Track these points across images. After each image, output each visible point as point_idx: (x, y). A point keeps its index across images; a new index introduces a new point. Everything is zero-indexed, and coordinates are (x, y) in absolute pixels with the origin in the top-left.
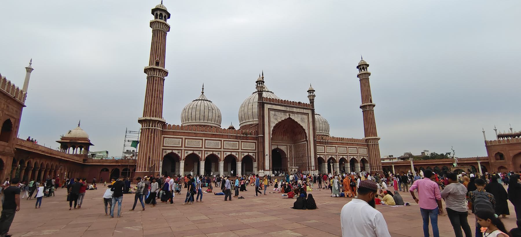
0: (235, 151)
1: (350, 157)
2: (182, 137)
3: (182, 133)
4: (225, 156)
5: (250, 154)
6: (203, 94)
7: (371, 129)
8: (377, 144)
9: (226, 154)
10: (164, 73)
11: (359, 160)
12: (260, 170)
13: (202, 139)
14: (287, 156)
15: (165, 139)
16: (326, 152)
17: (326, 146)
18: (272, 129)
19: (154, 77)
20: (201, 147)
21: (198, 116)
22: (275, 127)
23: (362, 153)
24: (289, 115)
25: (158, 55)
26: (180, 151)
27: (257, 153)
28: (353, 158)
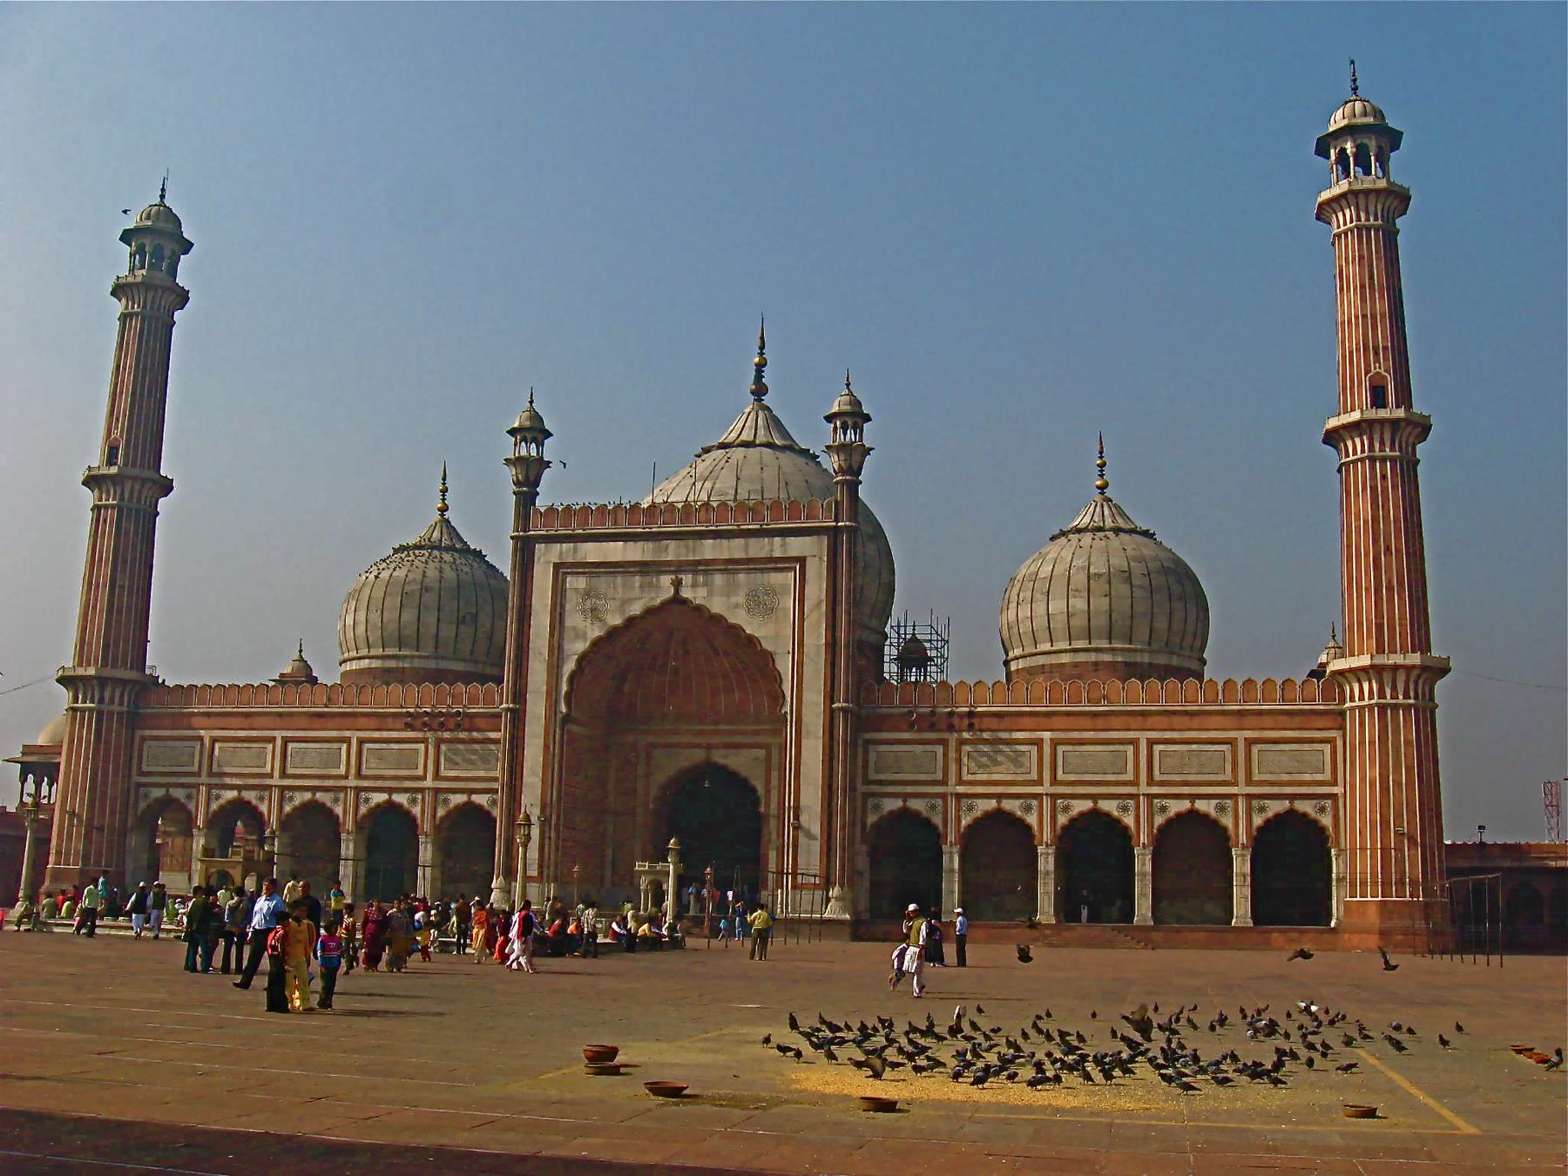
1: (1163, 809)
2: (202, 732)
5: (475, 798)
6: (442, 515)
8: (1395, 707)
9: (367, 800)
10: (137, 487)
11: (1240, 827)
13: (272, 740)
14: (762, 809)
17: (962, 742)
18: (569, 666)
20: (269, 771)
22: (583, 659)
23: (1286, 777)
24: (677, 584)
25: (117, 419)
28: (1192, 813)
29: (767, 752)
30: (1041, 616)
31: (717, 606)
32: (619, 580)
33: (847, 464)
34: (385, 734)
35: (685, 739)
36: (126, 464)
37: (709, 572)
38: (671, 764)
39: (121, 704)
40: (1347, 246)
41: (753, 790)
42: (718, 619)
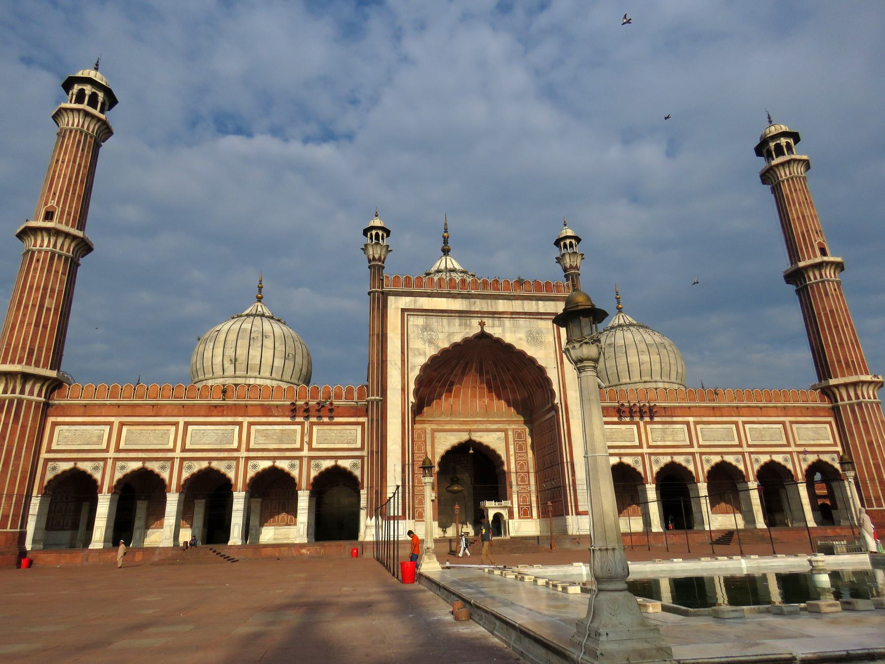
0: (288, 454)
1: (757, 460)
3: (111, 407)
4: (251, 473)
7: (835, 348)
8: (872, 403)
9: (255, 466)
11: (799, 469)
12: (369, 517)
14: (505, 468)
15: (57, 429)
16: (645, 445)
17: (646, 423)
18: (414, 374)
19: (33, 252)
20: (172, 448)
21: (218, 360)
22: (425, 368)
23: (812, 442)
24: (482, 324)
25: (55, 194)
26: (102, 463)
27: (366, 459)
29: (505, 434)
30: (624, 365)
31: (509, 338)
32: (445, 321)
33: (575, 265)
34: (271, 419)
35: (456, 427)
36: (60, 222)
37: (502, 319)
38: (446, 442)
39: (39, 395)
40: (789, 185)
41: (499, 457)
42: (510, 348)
